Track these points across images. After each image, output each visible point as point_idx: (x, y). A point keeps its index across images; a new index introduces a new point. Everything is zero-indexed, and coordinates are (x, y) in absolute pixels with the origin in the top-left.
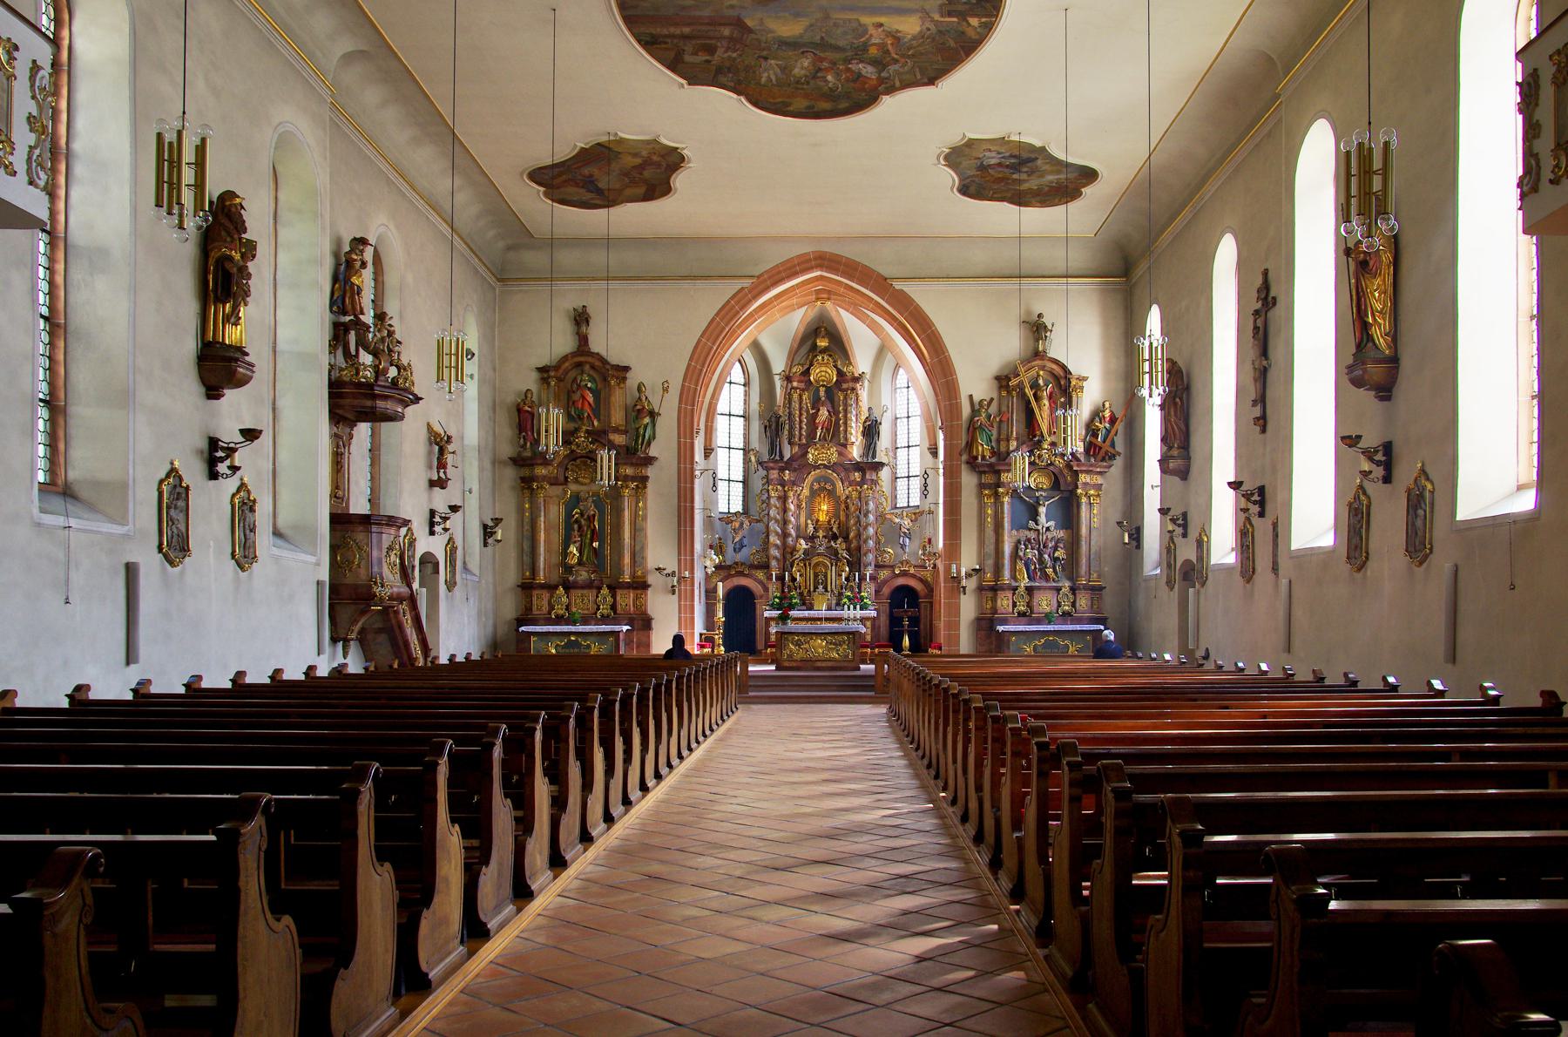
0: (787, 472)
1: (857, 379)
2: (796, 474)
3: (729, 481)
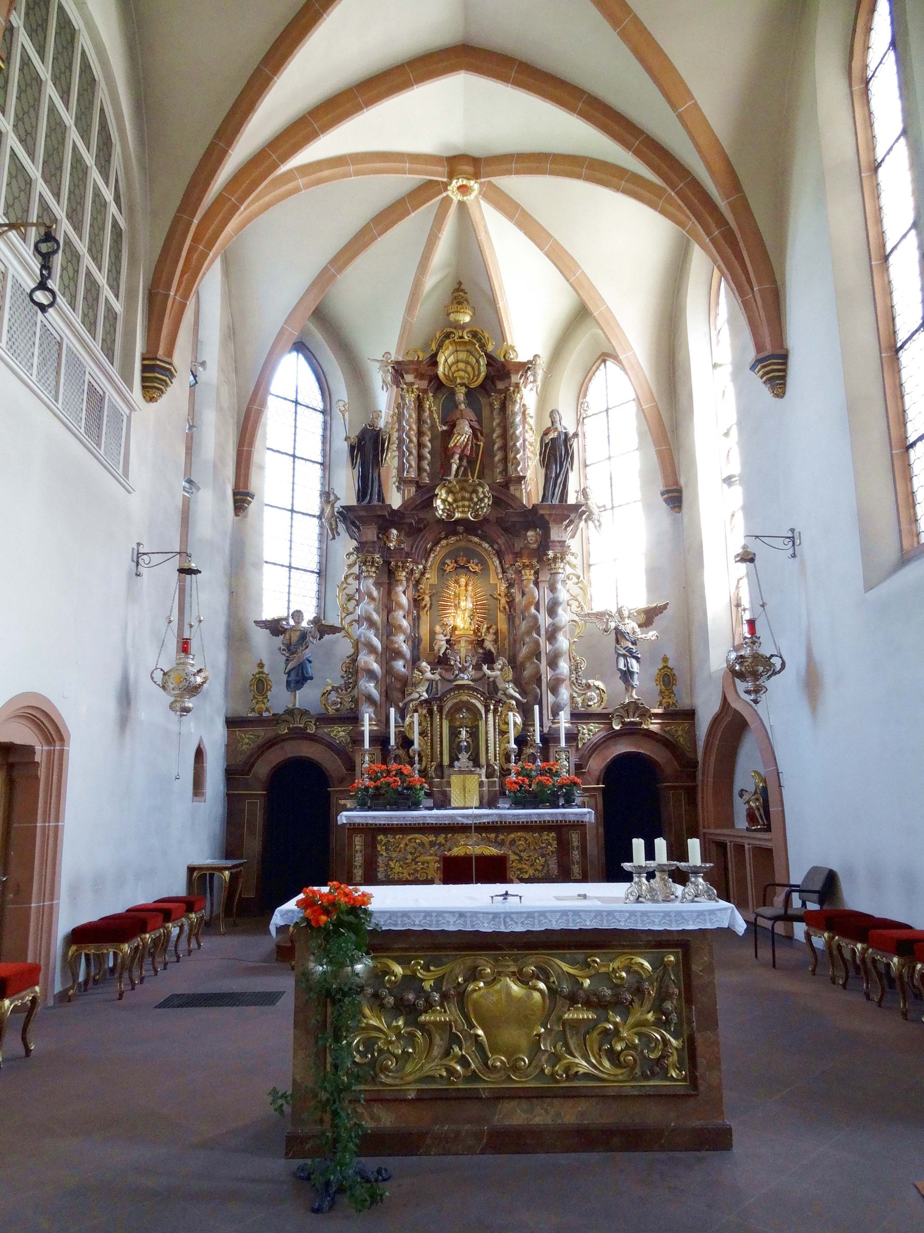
0: (394, 532)
1: (525, 367)
3: (290, 567)
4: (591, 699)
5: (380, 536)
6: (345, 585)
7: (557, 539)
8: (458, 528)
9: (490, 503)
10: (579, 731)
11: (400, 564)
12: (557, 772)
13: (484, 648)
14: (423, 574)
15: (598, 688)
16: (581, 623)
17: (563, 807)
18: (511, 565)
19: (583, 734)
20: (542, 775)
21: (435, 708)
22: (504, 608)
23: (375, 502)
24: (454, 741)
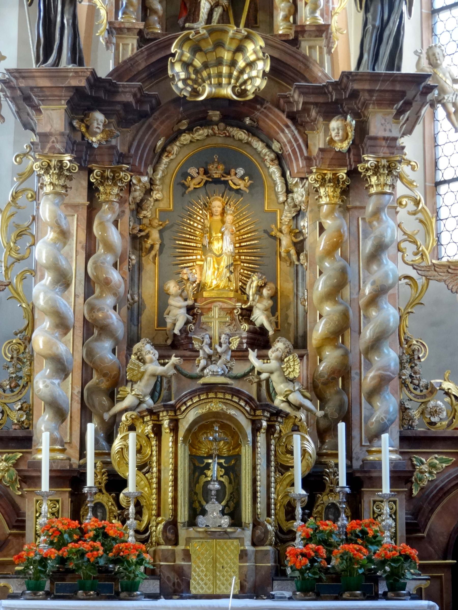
2: (129, 133)
4: (435, 412)
5: (75, 123)
6: (12, 209)
7: (382, 134)
8: (210, 113)
9: (268, 69)
10: (414, 466)
11: (108, 173)
12: (375, 537)
13: (251, 323)
14: (148, 192)
15: (447, 394)
16: (421, 281)
17: (385, 597)
18: (302, 179)
19: (422, 472)
20: (348, 541)
21: (166, 423)
22: (288, 252)
23: (64, 63)
24: (197, 482)
